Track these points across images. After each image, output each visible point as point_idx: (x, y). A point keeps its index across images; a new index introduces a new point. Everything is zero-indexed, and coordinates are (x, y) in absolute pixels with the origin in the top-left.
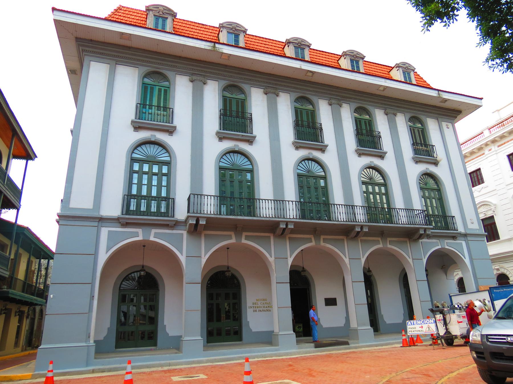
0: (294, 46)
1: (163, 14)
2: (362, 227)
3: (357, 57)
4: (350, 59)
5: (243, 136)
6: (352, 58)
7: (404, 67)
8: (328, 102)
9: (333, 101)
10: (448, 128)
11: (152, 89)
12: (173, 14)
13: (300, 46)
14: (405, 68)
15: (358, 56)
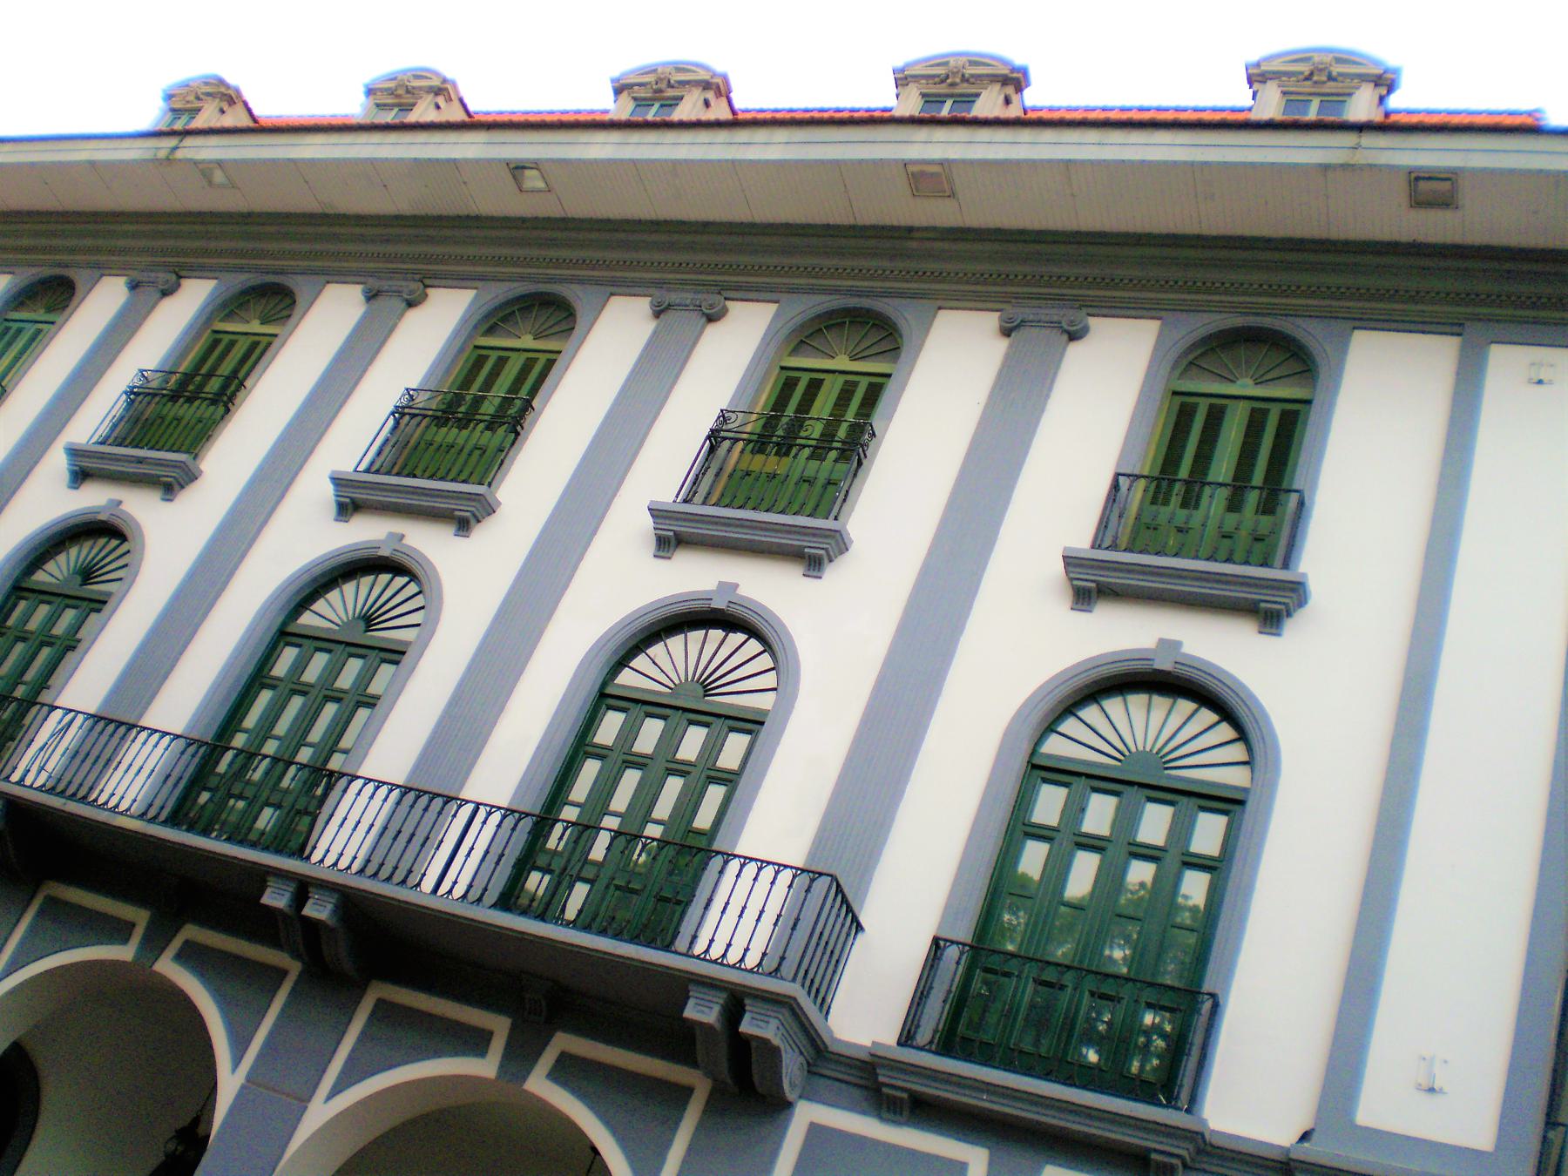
0: (635, 99)
1: (198, 98)
2: (303, 888)
3: (964, 79)
4: (924, 95)
5: (140, 461)
6: (942, 89)
7: (1302, 73)
8: (651, 302)
9: (673, 297)
10: (1540, 382)
11: (19, 331)
12: (223, 90)
13: (661, 91)
14: (1307, 79)
15: (969, 71)
